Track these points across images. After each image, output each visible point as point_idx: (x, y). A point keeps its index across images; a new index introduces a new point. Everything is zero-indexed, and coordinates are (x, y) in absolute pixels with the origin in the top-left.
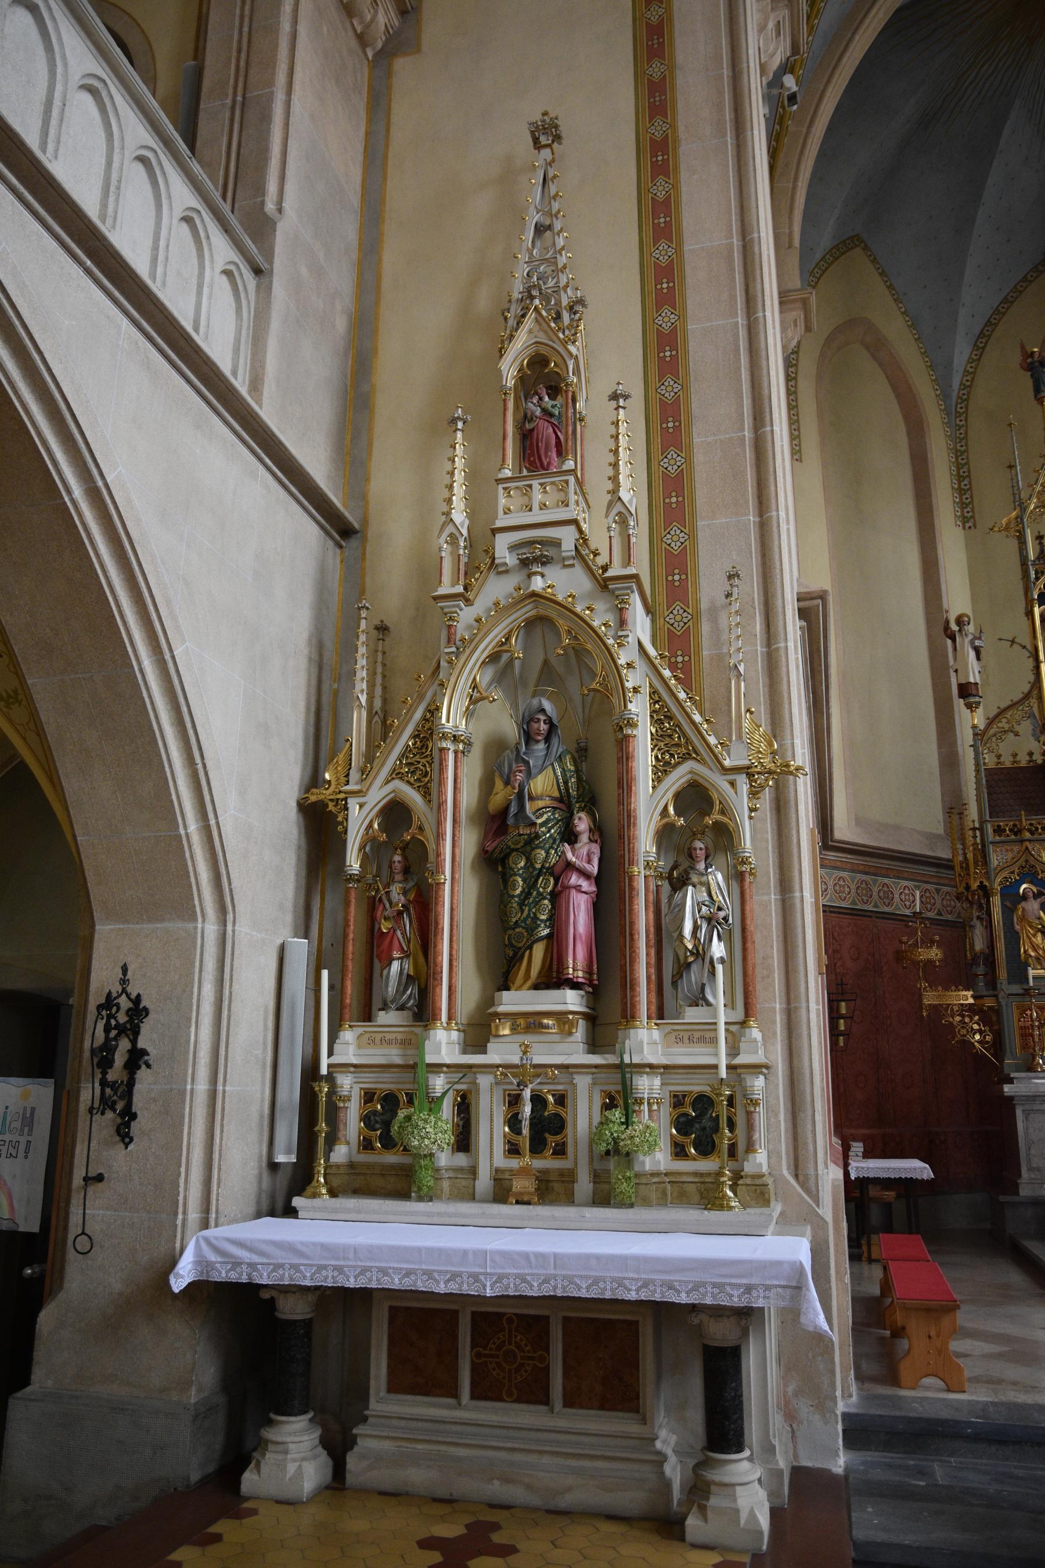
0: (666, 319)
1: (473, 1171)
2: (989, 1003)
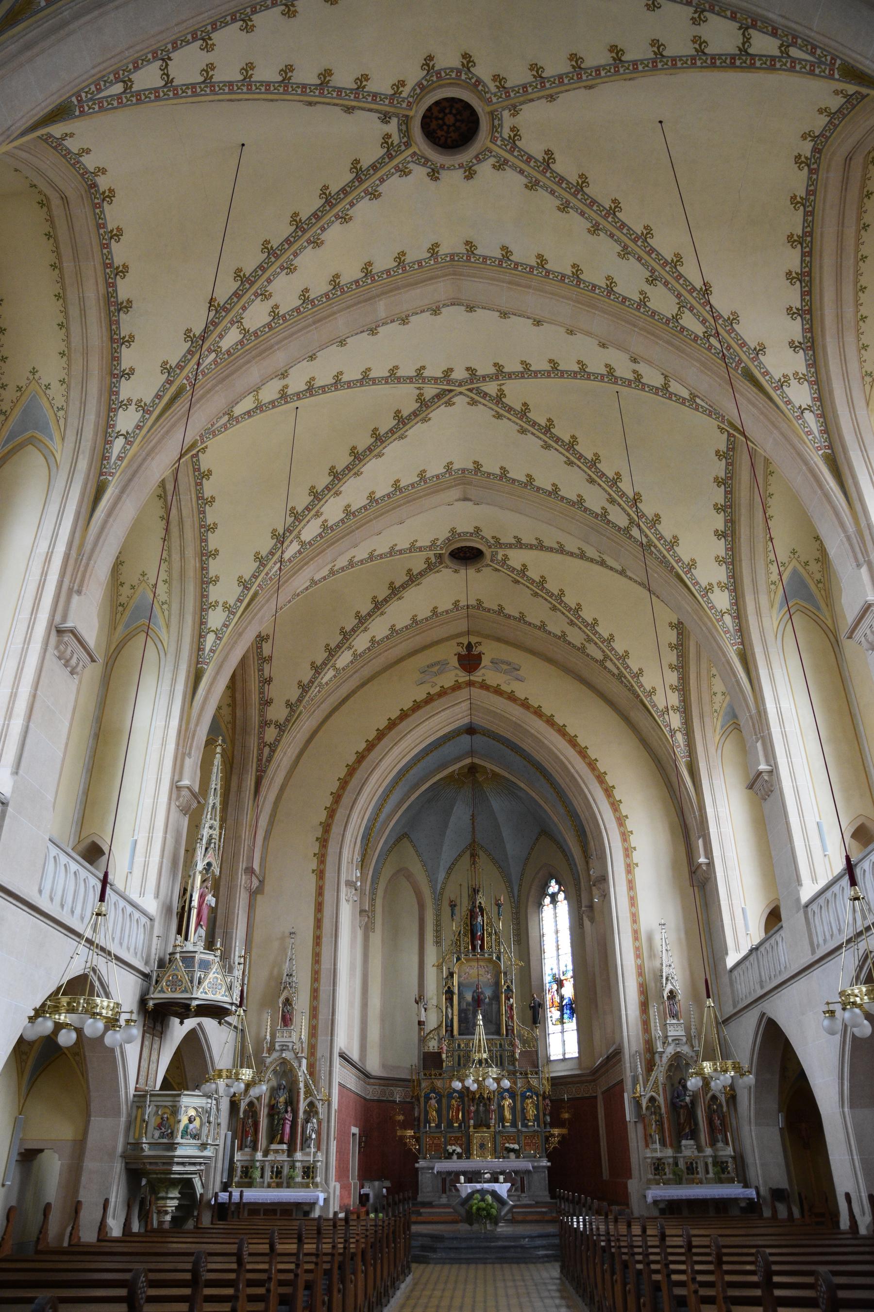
0: (316, 985)
1: (263, 1182)
2: (417, 1135)
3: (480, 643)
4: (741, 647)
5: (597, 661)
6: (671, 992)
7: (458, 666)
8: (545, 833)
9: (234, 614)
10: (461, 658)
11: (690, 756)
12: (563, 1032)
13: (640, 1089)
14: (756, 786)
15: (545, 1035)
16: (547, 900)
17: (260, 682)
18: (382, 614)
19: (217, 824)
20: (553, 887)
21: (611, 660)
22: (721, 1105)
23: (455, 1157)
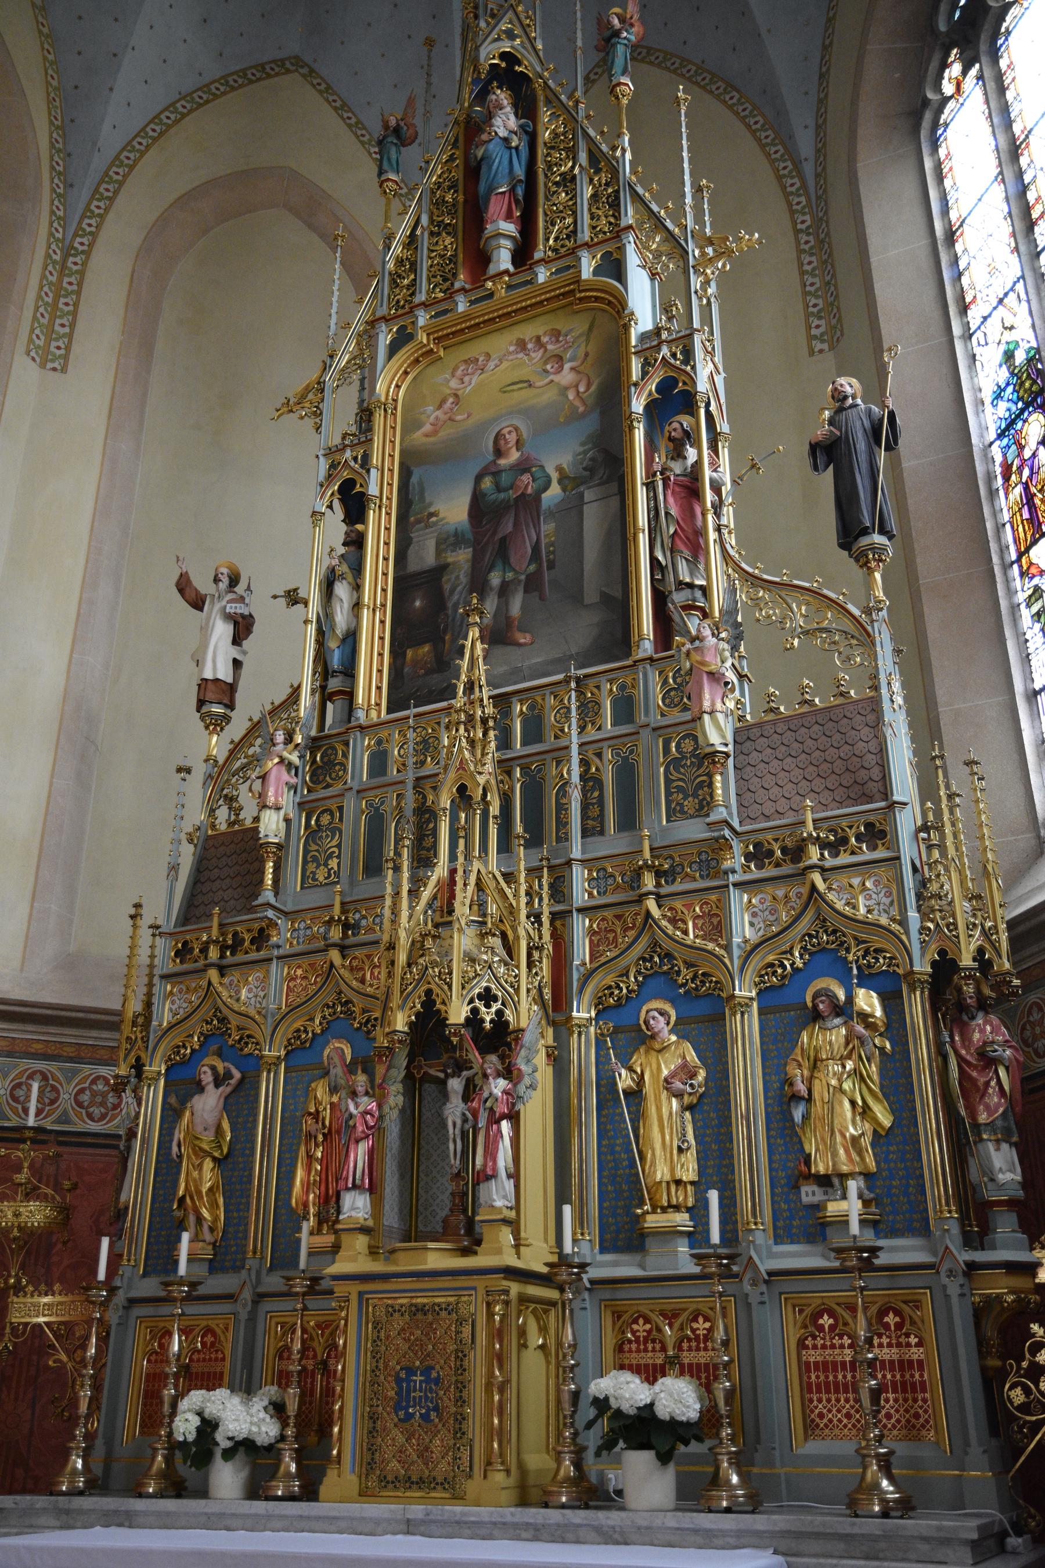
23: (227, 1478)
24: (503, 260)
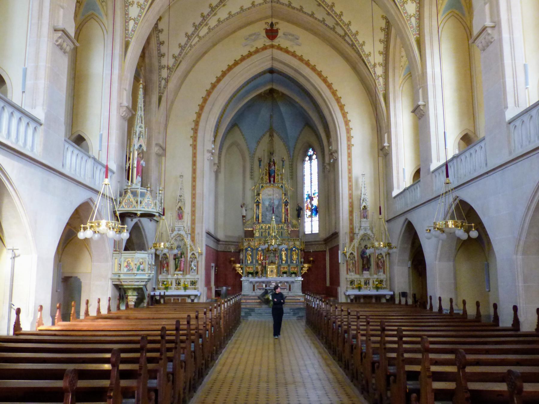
3: (277, 23)
4: (418, 36)
5: (340, 36)
6: (365, 206)
7: (265, 36)
8: (308, 124)
9: (144, 9)
10: (267, 31)
11: (385, 90)
12: (312, 221)
13: (347, 248)
14: (417, 111)
15: (304, 222)
16: (307, 158)
17: (157, 44)
18: (224, 5)
19: (143, 126)
20: (311, 152)
21: (348, 36)
22: (383, 257)
24: (272, 182)
